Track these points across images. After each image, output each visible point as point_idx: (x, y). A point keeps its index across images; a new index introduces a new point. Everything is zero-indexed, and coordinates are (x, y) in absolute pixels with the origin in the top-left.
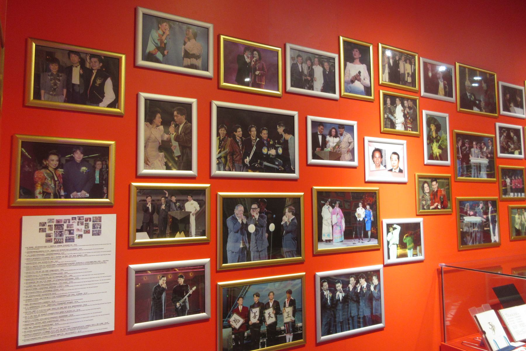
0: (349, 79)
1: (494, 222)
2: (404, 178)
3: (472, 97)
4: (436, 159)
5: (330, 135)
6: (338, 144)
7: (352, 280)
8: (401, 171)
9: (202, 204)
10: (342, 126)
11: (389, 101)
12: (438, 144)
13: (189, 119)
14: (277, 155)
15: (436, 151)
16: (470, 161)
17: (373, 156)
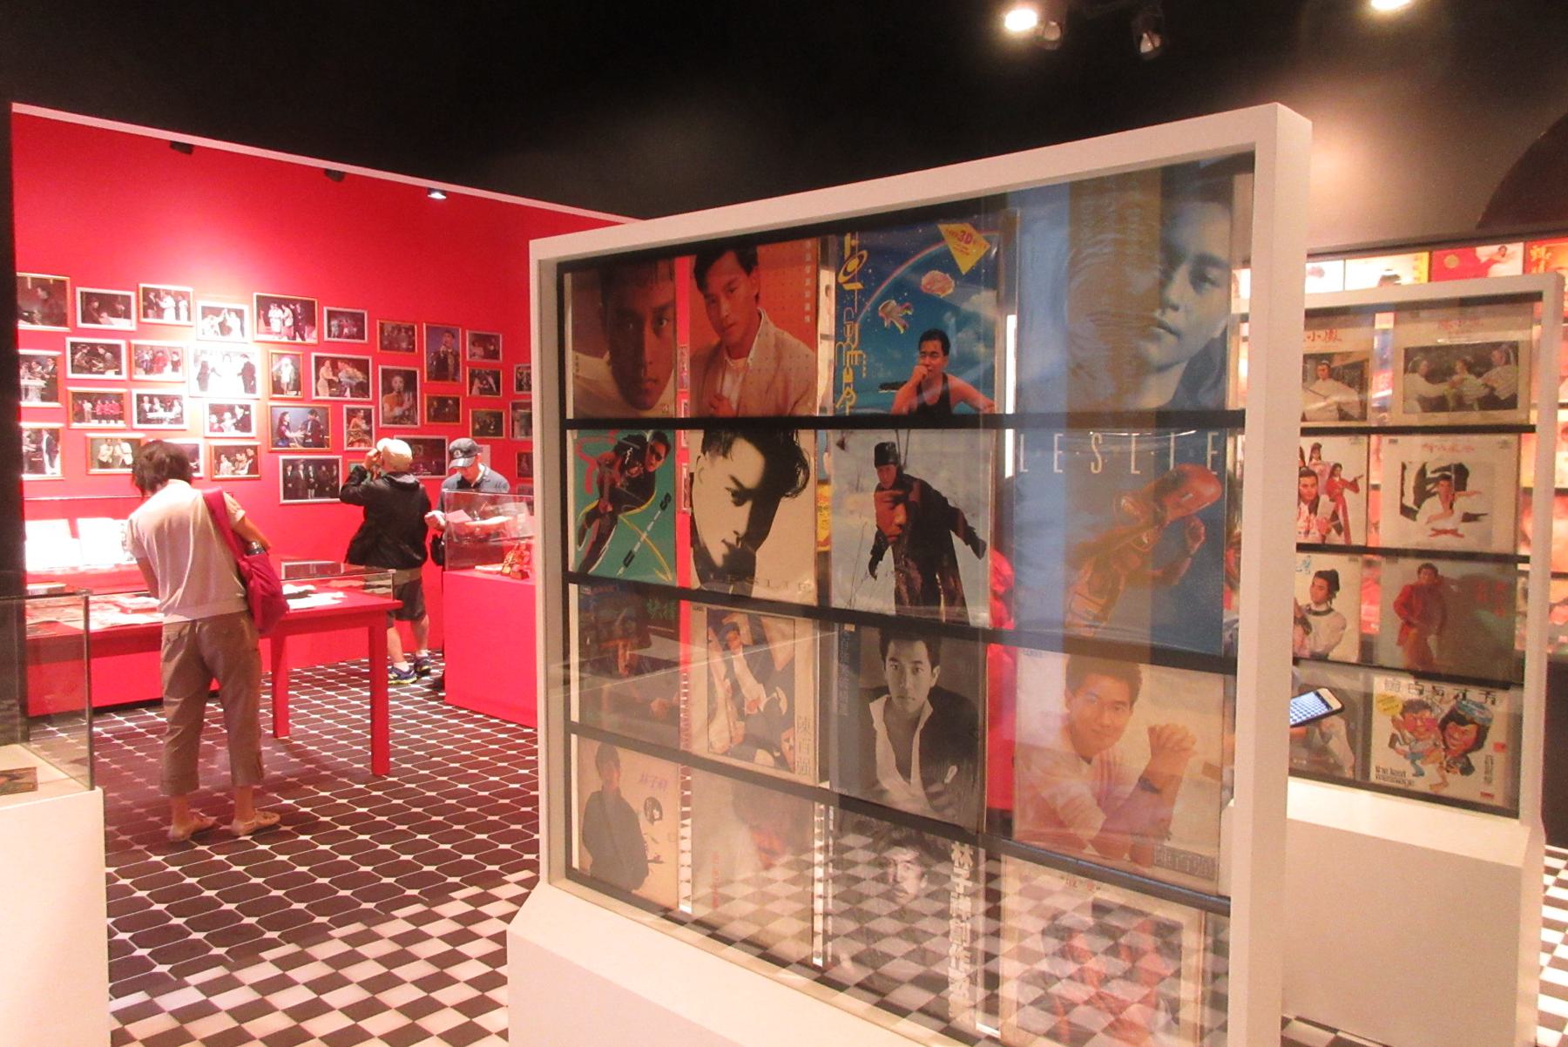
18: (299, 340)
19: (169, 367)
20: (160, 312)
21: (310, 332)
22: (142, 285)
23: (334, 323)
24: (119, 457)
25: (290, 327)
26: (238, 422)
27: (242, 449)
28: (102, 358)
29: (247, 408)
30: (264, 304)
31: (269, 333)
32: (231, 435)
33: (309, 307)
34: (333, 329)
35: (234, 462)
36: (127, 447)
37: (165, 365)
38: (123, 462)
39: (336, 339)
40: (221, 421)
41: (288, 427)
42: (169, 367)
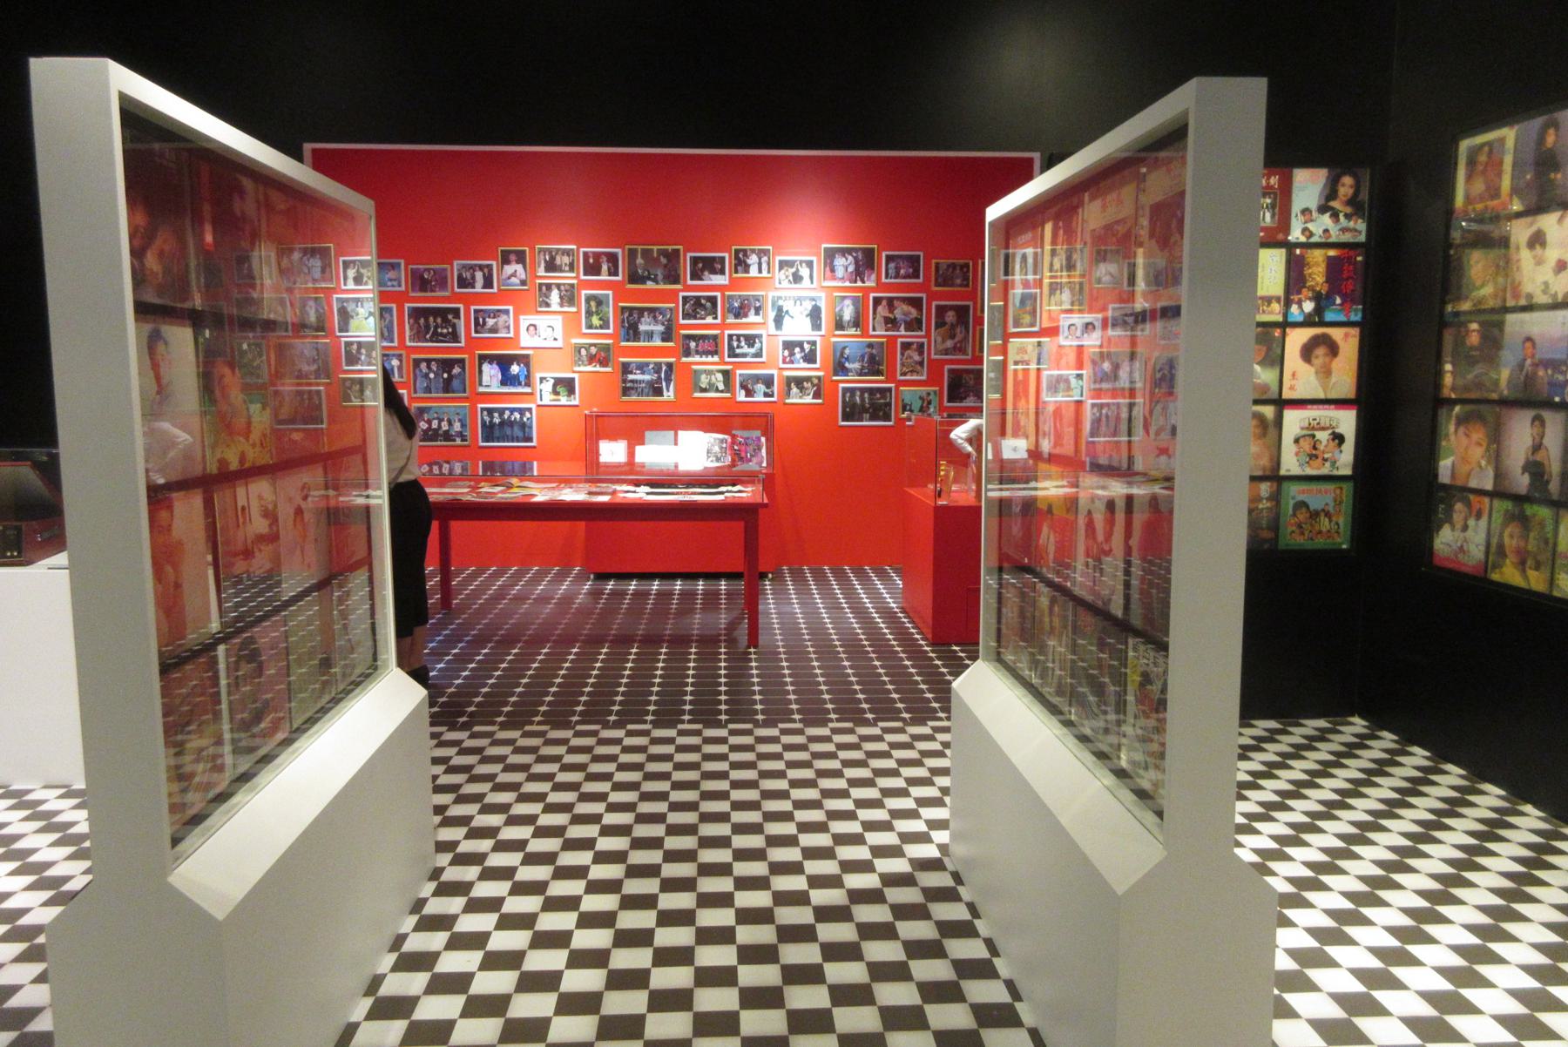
0: (504, 276)
1: (668, 380)
2: (559, 344)
4: (596, 328)
5: (489, 317)
6: (496, 323)
7: (507, 413)
8: (555, 339)
9: (401, 361)
10: (499, 311)
11: (544, 288)
13: (392, 316)
14: (448, 333)
17: (528, 329)
18: (859, 284)
19: (753, 311)
20: (747, 268)
21: (869, 276)
22: (734, 248)
23: (892, 265)
25: (852, 273)
26: (806, 355)
27: (808, 379)
28: (703, 306)
29: (814, 343)
30: (830, 255)
31: (834, 278)
32: (801, 369)
33: (869, 254)
34: (890, 271)
35: (802, 389)
36: (720, 377)
37: (749, 310)
39: (893, 281)
40: (792, 354)
41: (847, 359)
42: (753, 311)
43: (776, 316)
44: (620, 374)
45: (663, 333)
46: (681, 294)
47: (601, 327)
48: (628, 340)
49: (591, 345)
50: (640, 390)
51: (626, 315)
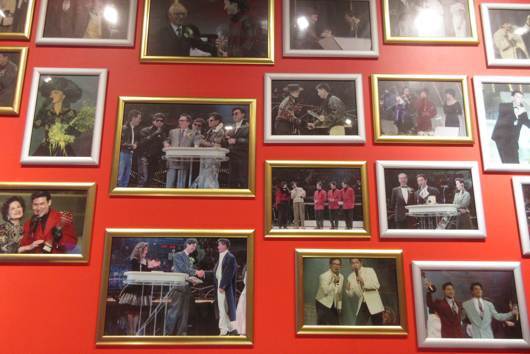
3: (188, 33)
4: (58, 152)
12: (66, 126)
15: (57, 138)
16: (164, 154)
19: (440, 117)
24: (356, 298)
37: (434, 114)
38: (364, 305)
42: (440, 117)
43: (497, 128)
44: (105, 267)
45: (224, 165)
46: (269, 78)
47: (70, 151)
48: (133, 183)
49: (37, 192)
50: (153, 314)
51: (136, 121)
